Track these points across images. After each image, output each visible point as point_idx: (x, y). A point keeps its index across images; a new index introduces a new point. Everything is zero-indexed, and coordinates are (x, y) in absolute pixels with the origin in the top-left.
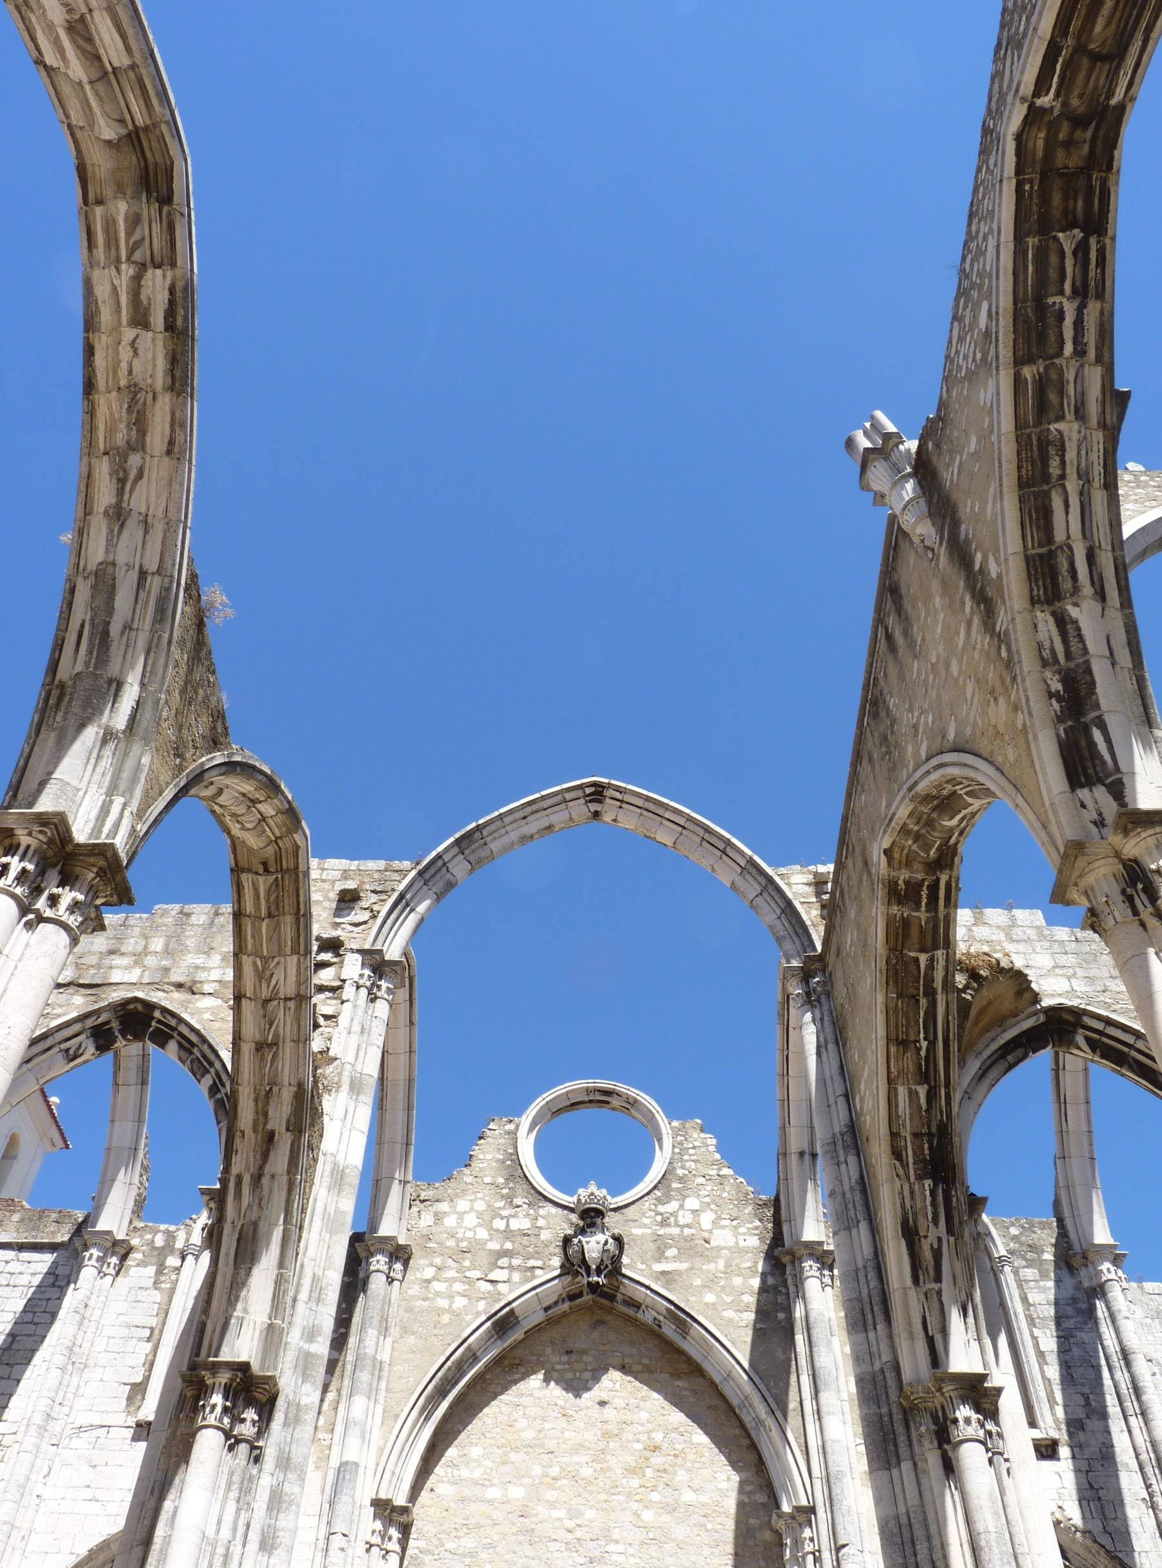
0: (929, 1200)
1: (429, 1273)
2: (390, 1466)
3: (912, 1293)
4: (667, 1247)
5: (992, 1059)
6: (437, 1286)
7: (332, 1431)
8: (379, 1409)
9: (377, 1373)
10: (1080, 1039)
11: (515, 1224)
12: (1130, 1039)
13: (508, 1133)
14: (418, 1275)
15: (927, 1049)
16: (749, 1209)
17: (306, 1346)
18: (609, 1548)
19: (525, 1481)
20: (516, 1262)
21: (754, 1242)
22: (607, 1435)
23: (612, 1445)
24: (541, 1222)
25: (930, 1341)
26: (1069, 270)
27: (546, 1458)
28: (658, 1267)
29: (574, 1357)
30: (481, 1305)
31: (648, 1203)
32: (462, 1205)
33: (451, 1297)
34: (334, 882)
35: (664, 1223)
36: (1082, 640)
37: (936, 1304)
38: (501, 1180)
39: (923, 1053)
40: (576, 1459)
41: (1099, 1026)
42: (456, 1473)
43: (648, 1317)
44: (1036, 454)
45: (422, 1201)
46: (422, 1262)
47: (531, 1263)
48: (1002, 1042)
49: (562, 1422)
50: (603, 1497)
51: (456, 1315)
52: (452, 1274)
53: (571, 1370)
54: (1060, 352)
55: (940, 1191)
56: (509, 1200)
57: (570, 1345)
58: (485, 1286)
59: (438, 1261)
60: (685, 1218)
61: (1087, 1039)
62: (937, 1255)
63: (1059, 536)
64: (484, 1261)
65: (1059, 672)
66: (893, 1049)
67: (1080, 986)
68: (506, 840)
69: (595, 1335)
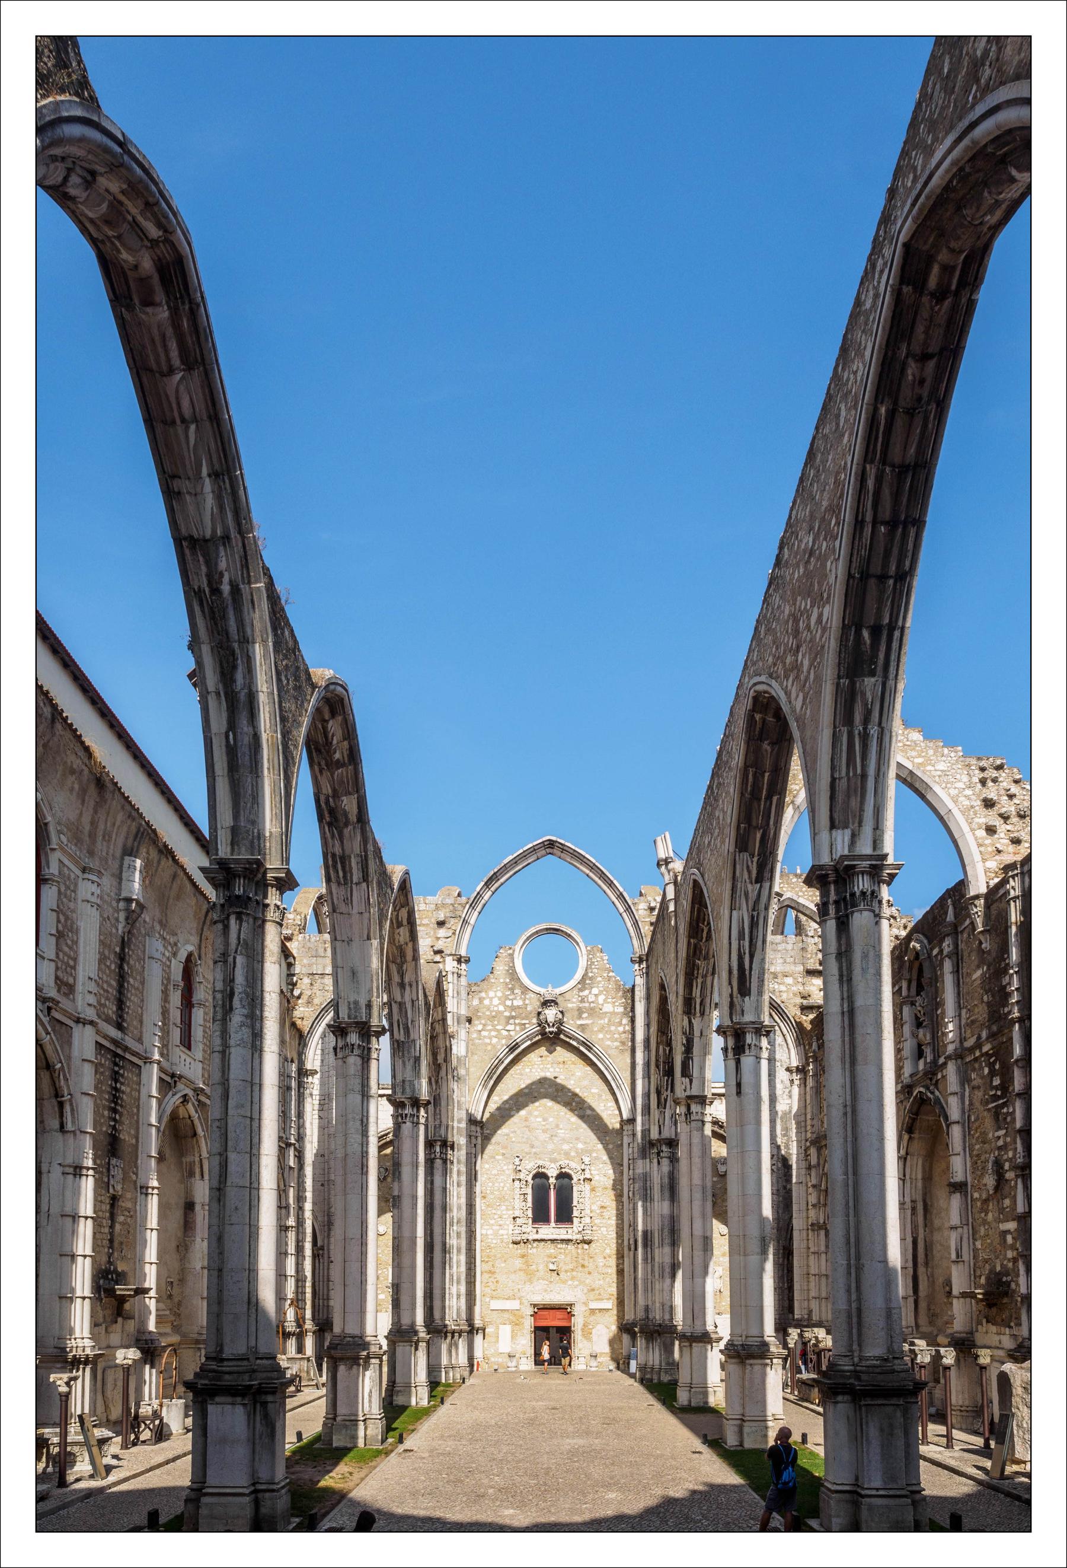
1: (480, 1027)
4: (583, 1012)
6: (484, 1033)
11: (516, 1003)
16: (621, 993)
20: (517, 1021)
21: (621, 1009)
24: (527, 1002)
28: (579, 1022)
30: (504, 1041)
31: (575, 991)
32: (491, 994)
33: (490, 1038)
35: (582, 1001)
43: (575, 1043)
46: (477, 1022)
47: (524, 1022)
51: (494, 1046)
52: (490, 1027)
56: (512, 990)
58: (505, 1033)
60: (591, 998)
64: (503, 1021)
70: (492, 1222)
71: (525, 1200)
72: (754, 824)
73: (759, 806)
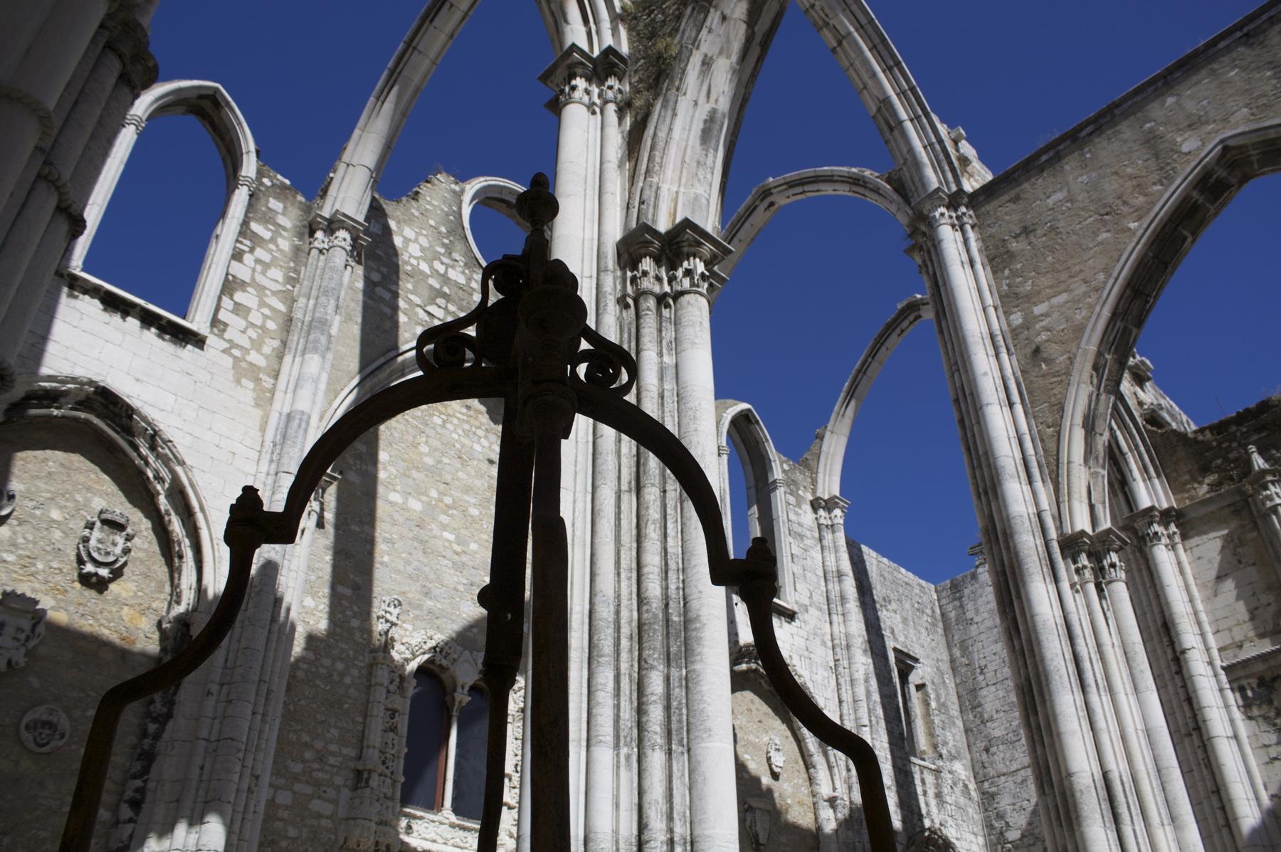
7: (276, 377)
11: (452, 274)
13: (454, 192)
19: (424, 498)
27: (442, 486)
29: (471, 413)
38: (443, 229)
40: (466, 498)
42: (364, 467)
49: (457, 464)
53: (468, 422)
56: (449, 250)
59: (384, 270)
64: (426, 293)
66: (1128, 292)
70: (297, 768)
71: (393, 729)
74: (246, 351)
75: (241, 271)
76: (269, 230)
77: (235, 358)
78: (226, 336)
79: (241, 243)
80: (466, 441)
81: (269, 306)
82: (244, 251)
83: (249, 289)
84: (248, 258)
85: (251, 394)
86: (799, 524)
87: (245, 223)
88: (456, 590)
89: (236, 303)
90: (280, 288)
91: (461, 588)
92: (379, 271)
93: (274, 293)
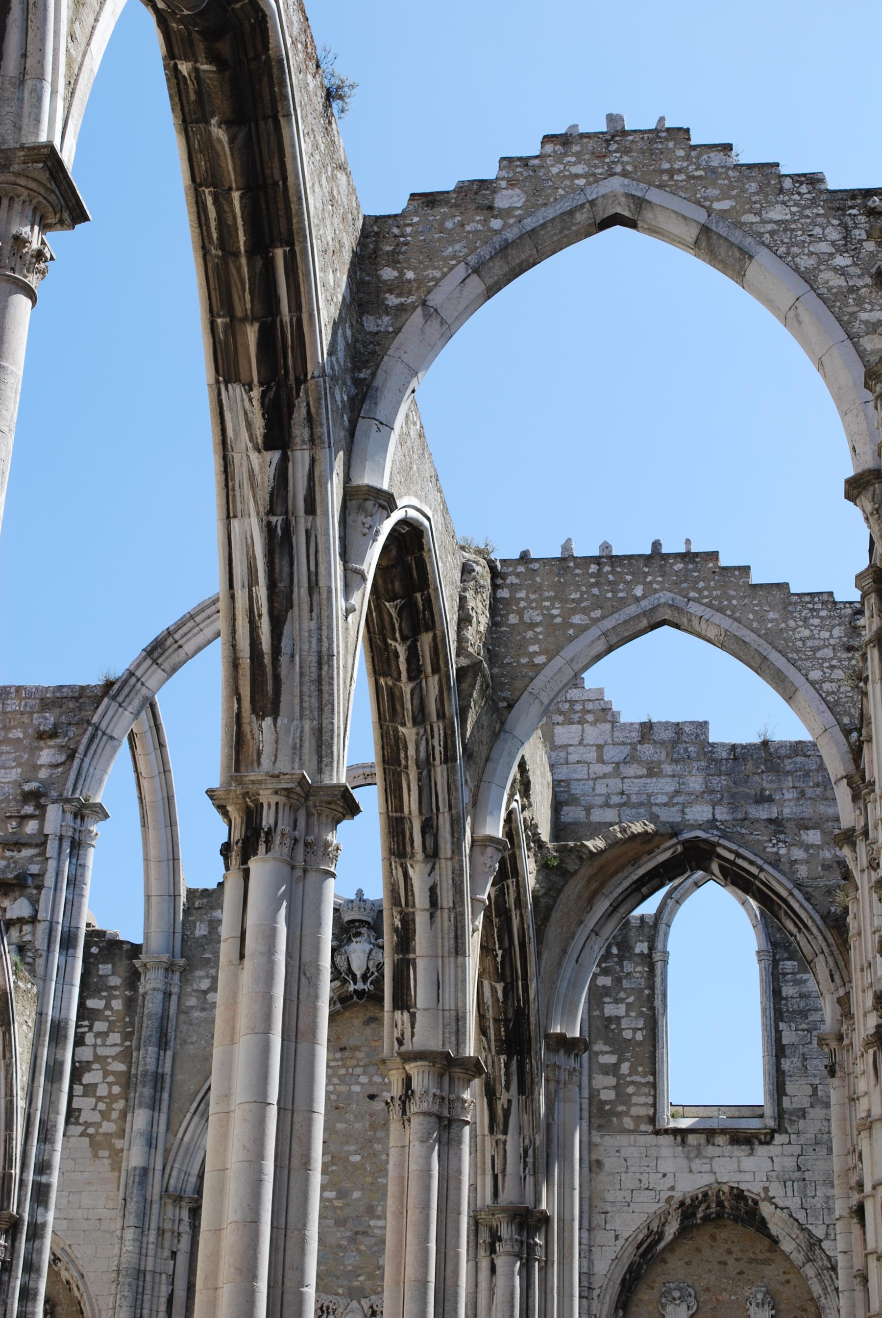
0: (503, 1071)
2: (177, 1165)
3: (488, 1139)
5: (625, 894)
7: (123, 1137)
8: (163, 1117)
9: (159, 1085)
10: (715, 867)
12: (754, 870)
14: (195, 987)
15: (503, 956)
17: (38, 1178)
18: (372, 1223)
22: (373, 1127)
23: (379, 1134)
25: (495, 1177)
26: (397, 626)
34: (31, 714)
36: (413, 895)
37: (501, 1151)
39: (499, 959)
40: (346, 1148)
41: (731, 857)
44: (393, 742)
45: (196, 909)
46: (199, 973)
48: (635, 877)
50: (369, 1180)
53: (344, 1066)
54: (399, 679)
55: (514, 1062)
57: (344, 1043)
61: (721, 867)
62: (507, 1113)
63: (406, 810)
65: (401, 913)
67: (722, 813)
68: (200, 639)
69: (368, 1031)
72: (239, 314)
73: (239, 269)
74: (98, 1125)
75: (86, 1054)
76: (101, 998)
77: (90, 1136)
78: (81, 1121)
79: (81, 1026)
80: (342, 1088)
81: (113, 1073)
82: (84, 1033)
83: (95, 1066)
84: (89, 1039)
85: (107, 1162)
86: (802, 996)
87: (81, 1005)
88: (339, 1246)
89: (85, 1086)
90: (119, 1049)
91: (344, 1243)
92: (207, 977)
93: (114, 1058)
